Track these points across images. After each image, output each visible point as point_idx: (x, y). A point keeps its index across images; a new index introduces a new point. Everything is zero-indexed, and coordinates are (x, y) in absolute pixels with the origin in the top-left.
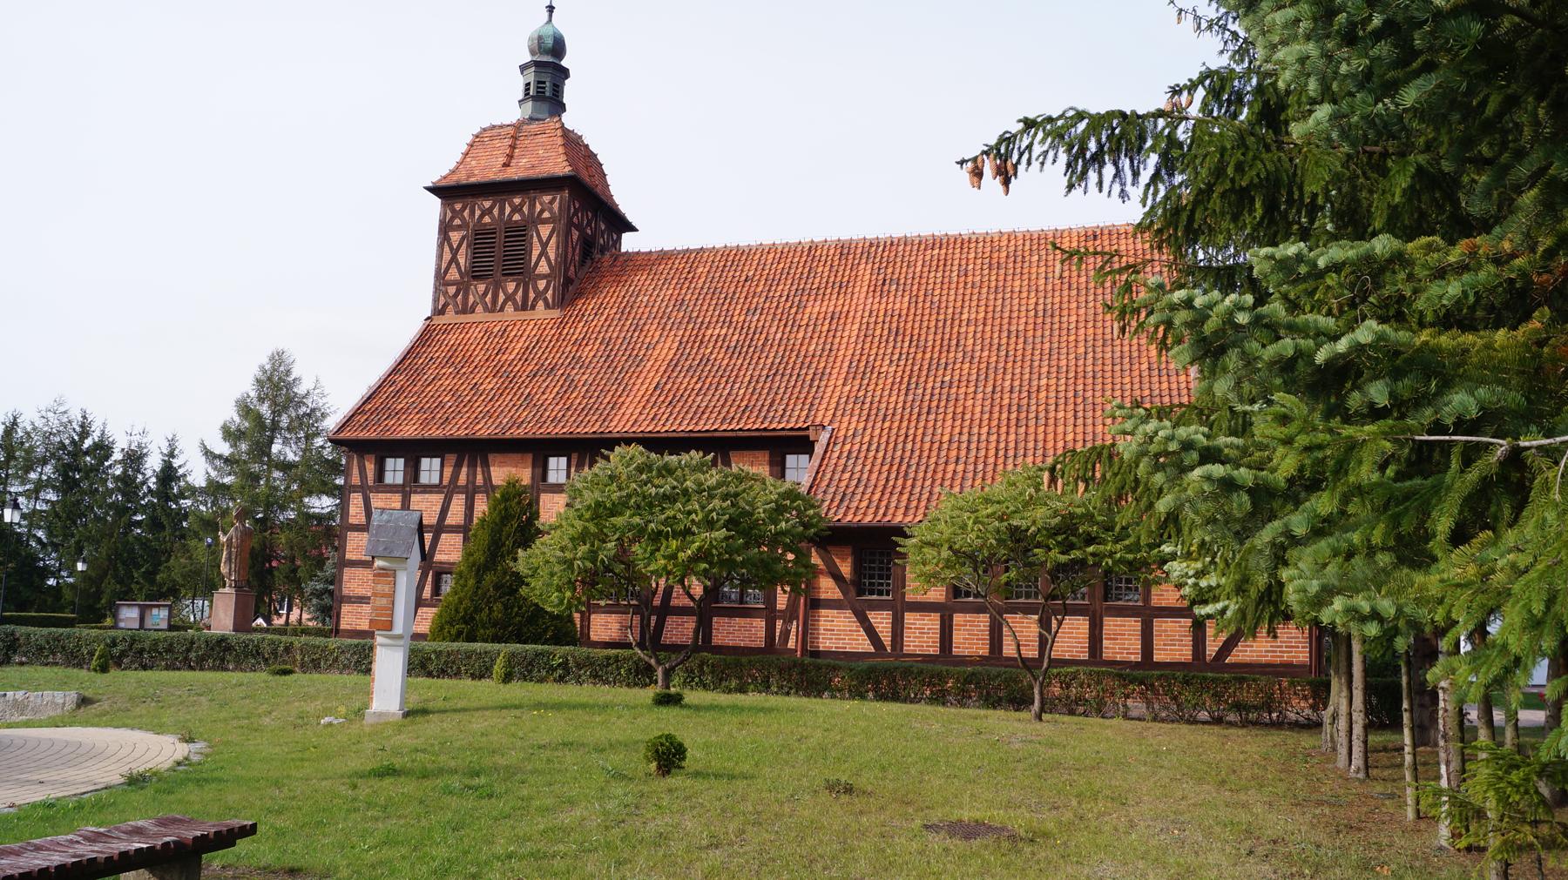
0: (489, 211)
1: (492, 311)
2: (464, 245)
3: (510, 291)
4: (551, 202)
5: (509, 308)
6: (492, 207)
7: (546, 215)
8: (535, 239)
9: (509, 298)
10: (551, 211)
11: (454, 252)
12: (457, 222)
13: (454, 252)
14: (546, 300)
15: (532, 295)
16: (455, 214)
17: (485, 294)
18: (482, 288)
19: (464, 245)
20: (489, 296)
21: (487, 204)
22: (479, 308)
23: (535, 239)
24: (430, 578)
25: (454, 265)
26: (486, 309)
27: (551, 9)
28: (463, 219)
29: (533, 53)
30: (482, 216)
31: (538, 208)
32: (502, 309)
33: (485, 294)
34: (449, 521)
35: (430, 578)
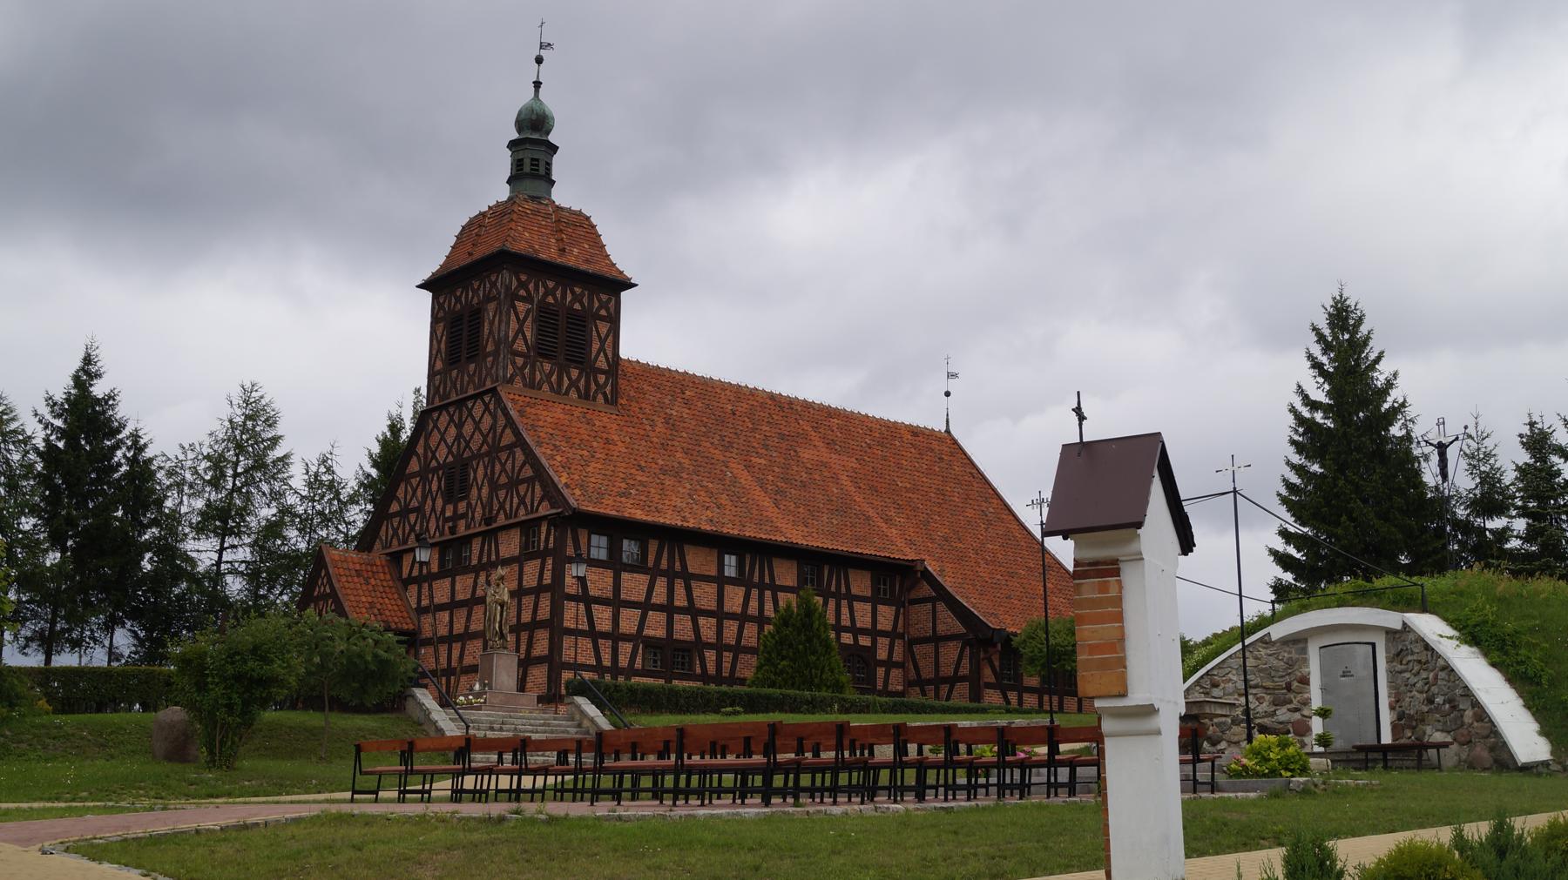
0: (553, 293)
1: (558, 393)
2: (530, 319)
3: (574, 378)
4: (610, 300)
5: (573, 395)
6: (555, 289)
7: (603, 312)
8: (594, 333)
9: (573, 384)
10: (607, 310)
11: (521, 323)
12: (522, 292)
13: (521, 323)
14: (605, 394)
15: (593, 387)
16: (522, 285)
17: (551, 373)
18: (547, 367)
19: (530, 319)
20: (554, 377)
21: (551, 284)
22: (546, 387)
23: (594, 333)
24: (640, 651)
25: (520, 336)
26: (552, 389)
27: (537, 84)
28: (528, 291)
29: (520, 128)
30: (546, 295)
31: (596, 305)
32: (567, 393)
33: (551, 373)
34: (654, 600)
35: (640, 651)
